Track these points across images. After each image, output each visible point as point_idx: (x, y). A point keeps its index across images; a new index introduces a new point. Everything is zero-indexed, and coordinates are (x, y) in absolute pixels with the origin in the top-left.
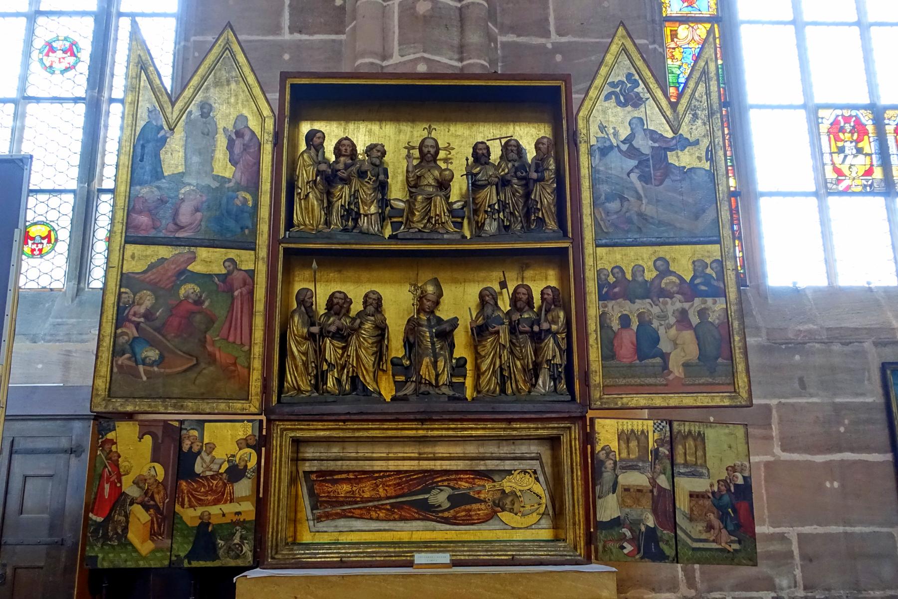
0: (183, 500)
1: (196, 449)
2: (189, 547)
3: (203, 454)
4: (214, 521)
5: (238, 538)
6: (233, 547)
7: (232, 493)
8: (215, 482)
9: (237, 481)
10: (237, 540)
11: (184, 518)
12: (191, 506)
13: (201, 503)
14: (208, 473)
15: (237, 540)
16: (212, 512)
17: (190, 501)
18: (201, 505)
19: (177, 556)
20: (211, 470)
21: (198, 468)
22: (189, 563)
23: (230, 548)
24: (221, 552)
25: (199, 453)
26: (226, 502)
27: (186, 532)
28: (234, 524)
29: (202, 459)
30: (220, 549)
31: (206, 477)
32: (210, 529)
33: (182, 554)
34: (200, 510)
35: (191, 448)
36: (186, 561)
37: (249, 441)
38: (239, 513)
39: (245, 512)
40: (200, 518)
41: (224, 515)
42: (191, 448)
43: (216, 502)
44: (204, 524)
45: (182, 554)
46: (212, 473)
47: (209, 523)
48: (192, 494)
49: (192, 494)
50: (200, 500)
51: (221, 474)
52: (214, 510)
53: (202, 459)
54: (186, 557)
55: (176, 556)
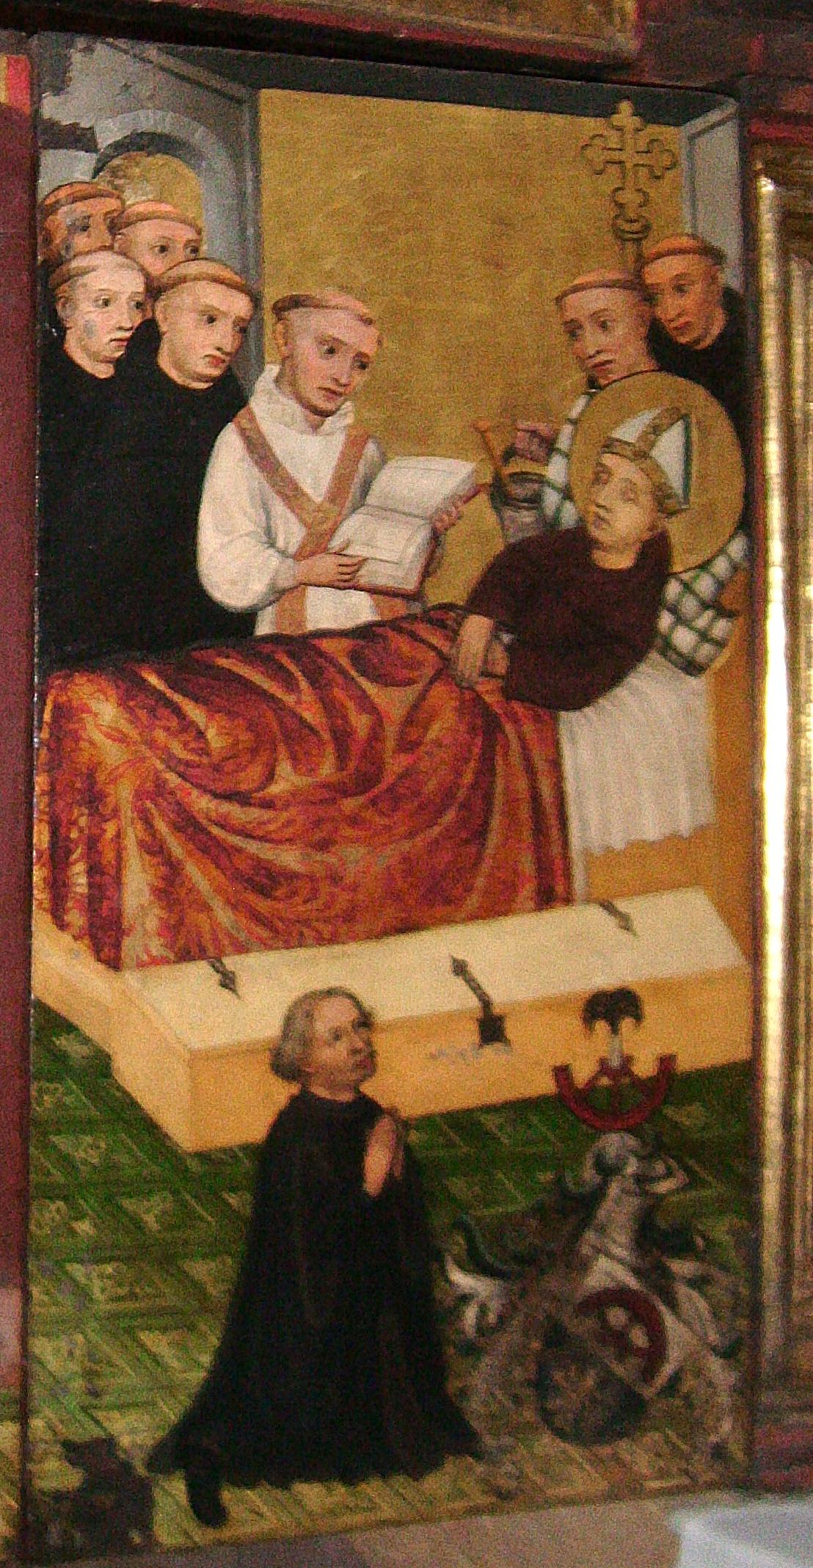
0: (106, 879)
1: (192, 352)
2: (187, 1361)
3: (268, 406)
4: (417, 1082)
5: (621, 1242)
6: (582, 1327)
7: (547, 819)
8: (393, 702)
9: (583, 697)
10: (610, 1267)
11: (136, 1073)
12: (186, 945)
13: (283, 910)
14: (331, 611)
15: (610, 1267)
16: (389, 1003)
17: (170, 888)
18: (283, 934)
19: (93, 1454)
20: (347, 581)
21: (235, 553)
22: (207, 1509)
23: (555, 1337)
24: (480, 1387)
25: (227, 397)
26: (497, 905)
27: (151, 1212)
28: (579, 1106)
29: (259, 451)
30: (472, 1350)
31: (304, 647)
32: (378, 1163)
33: (135, 1432)
34: (271, 986)
35: (146, 338)
36: (172, 1494)
37: (670, 308)
38: (613, 1006)
39: (661, 988)
40: (284, 1066)
41: (491, 1028)
42: (146, 338)
43: (420, 900)
44: (321, 1127)
45: (135, 1432)
46: (358, 609)
47: (367, 1111)
48: (187, 824)
49: (187, 824)
50: (265, 880)
51: (445, 619)
52: (407, 978)
53: (259, 451)
54: (180, 1450)
55: (74, 1452)
